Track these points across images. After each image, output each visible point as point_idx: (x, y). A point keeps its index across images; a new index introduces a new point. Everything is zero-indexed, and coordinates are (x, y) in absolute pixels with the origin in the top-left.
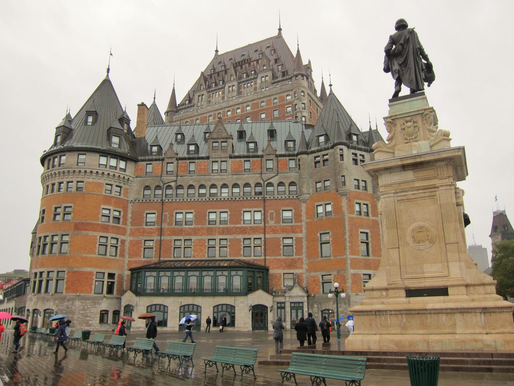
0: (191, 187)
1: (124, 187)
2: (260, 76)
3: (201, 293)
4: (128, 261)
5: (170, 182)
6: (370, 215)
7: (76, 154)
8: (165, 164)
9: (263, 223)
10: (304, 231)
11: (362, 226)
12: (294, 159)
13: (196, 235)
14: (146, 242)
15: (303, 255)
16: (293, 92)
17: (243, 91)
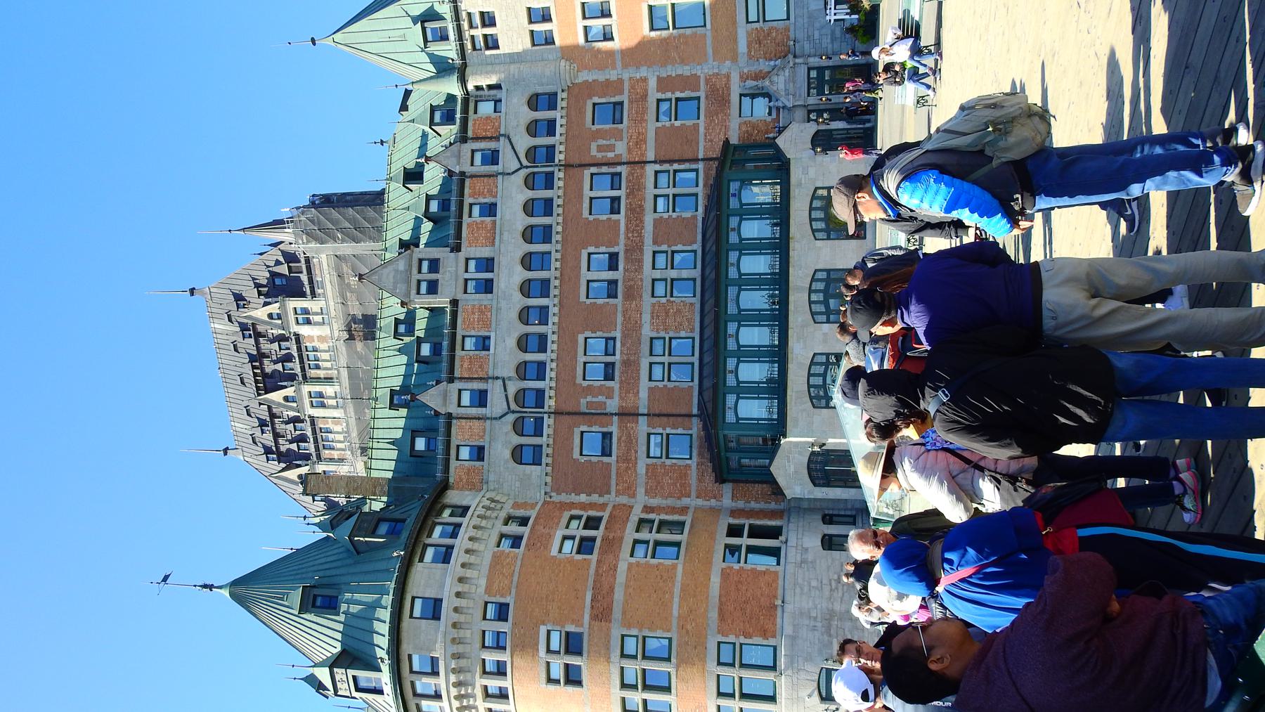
0: (523, 344)
1: (508, 509)
2: (295, 328)
3: (779, 281)
4: (697, 497)
5: (506, 396)
7: (406, 622)
8: (461, 411)
9: (618, 169)
10: (643, 72)
12: (476, 102)
14: (652, 454)
15: (699, 74)
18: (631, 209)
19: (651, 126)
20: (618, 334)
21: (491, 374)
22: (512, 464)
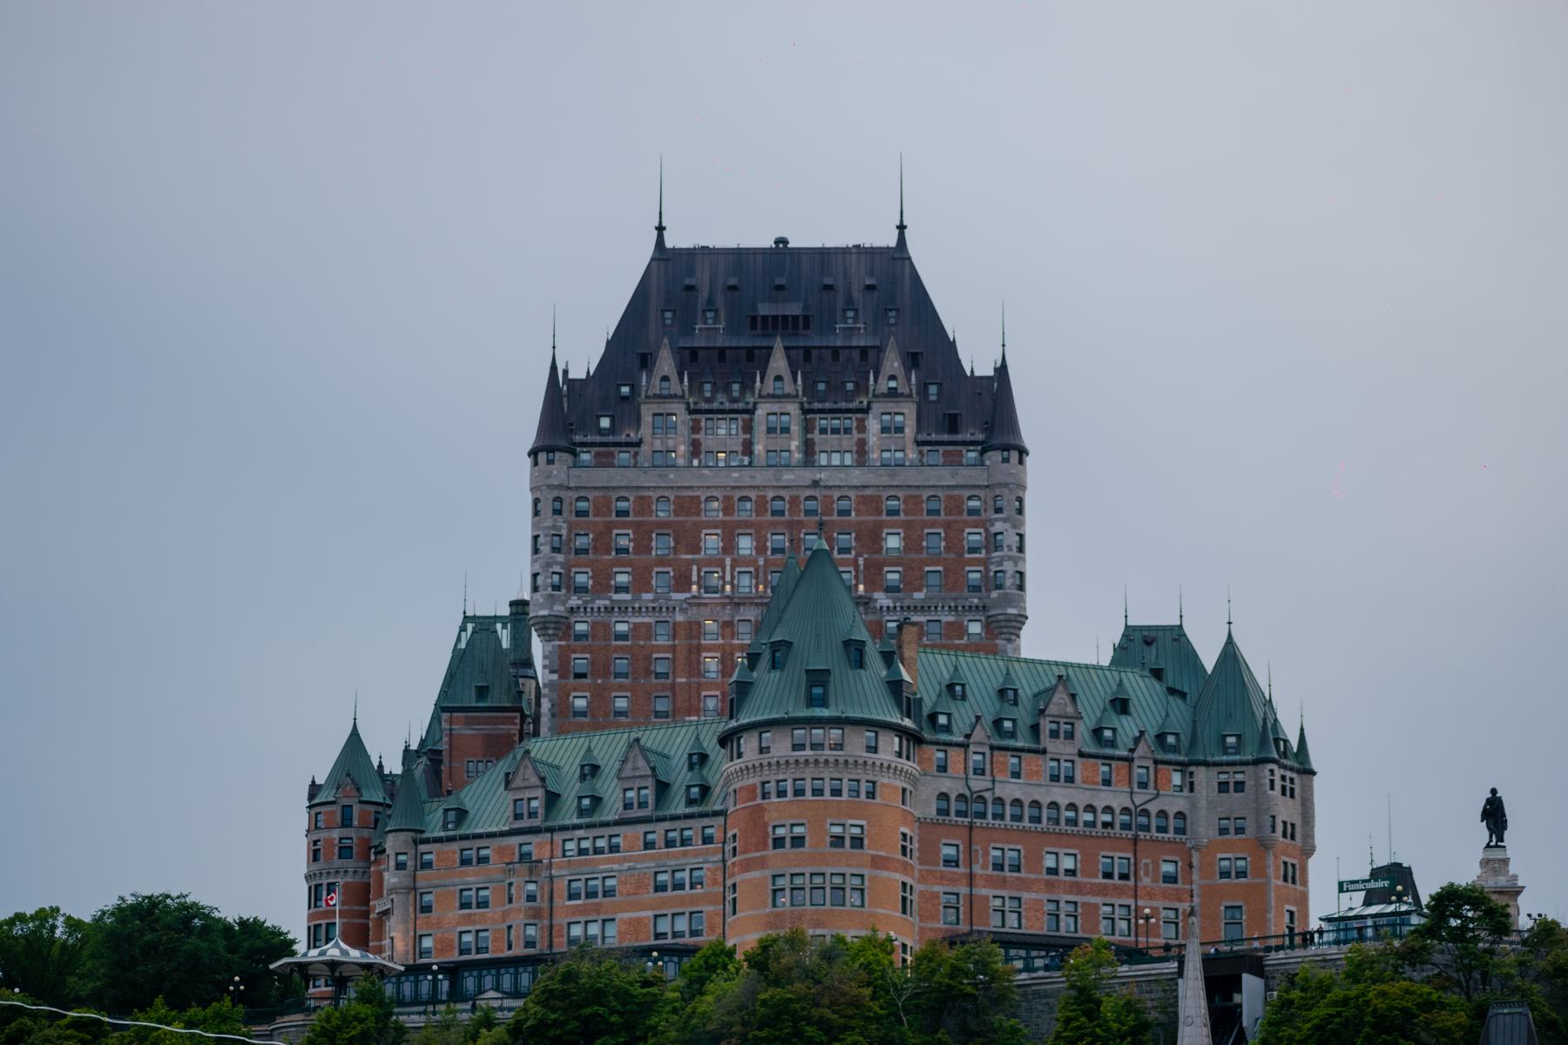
0: (1017, 802)
2: (877, 408)
4: (920, 928)
6: (1298, 882)
8: (971, 753)
9: (1132, 879)
11: (1288, 901)
12: (1181, 771)
13: (1028, 891)
17: (816, 440)
18: (1105, 886)
20: (1023, 874)
21: (997, 778)
22: (937, 793)
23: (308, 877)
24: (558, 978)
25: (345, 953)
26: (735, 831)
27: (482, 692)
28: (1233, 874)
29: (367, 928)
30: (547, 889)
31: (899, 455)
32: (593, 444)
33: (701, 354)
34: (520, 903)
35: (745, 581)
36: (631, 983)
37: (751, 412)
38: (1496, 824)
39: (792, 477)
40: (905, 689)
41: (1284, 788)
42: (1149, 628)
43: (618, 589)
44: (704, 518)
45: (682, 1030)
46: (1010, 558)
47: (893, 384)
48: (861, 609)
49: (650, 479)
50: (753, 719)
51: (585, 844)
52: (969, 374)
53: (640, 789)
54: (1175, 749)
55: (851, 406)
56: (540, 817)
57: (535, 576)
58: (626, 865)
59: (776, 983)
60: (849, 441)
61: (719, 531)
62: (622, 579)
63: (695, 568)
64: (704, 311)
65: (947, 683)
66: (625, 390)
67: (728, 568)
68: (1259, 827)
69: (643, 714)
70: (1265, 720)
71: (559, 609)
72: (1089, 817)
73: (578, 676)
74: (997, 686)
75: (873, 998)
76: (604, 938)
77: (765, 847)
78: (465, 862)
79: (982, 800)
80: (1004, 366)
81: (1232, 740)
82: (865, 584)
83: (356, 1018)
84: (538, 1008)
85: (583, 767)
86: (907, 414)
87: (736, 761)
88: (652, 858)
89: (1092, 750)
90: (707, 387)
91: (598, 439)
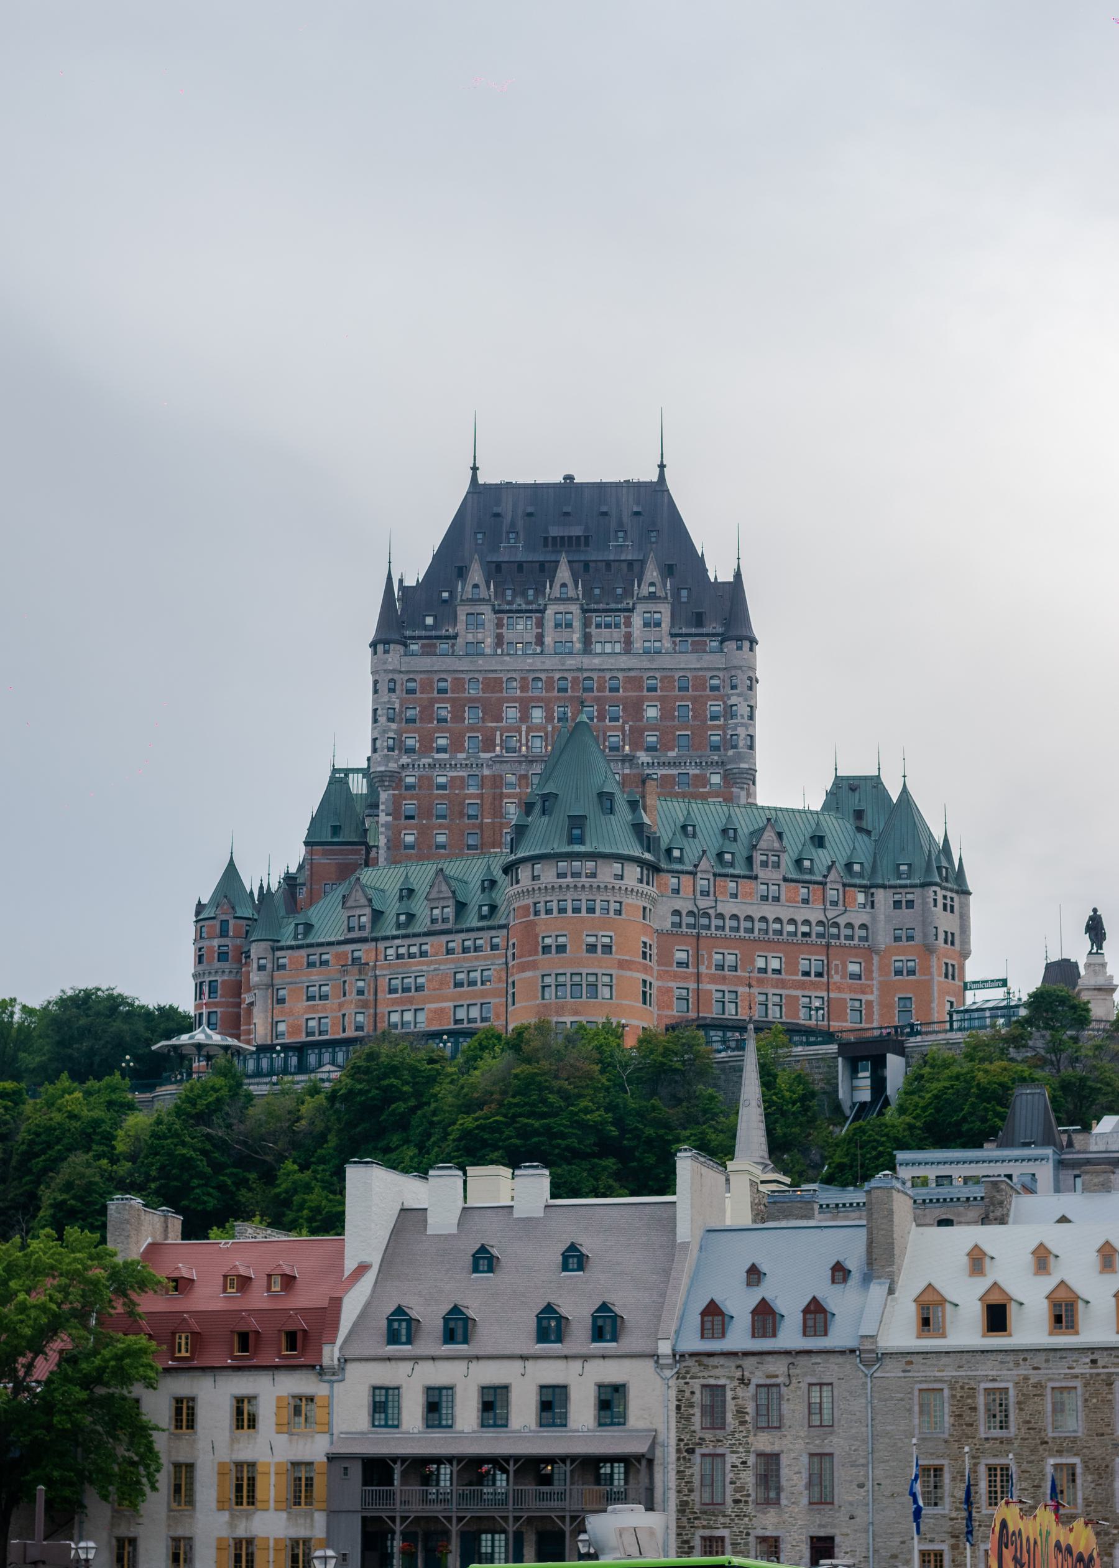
0: (734, 917)
2: (640, 608)
10: (876, 992)
11: (948, 994)
16: (727, 676)
18: (804, 982)
19: (847, 996)
20: (739, 973)
23: (195, 976)
24: (363, 1057)
25: (208, 1037)
26: (514, 940)
27: (336, 830)
28: (905, 973)
29: (238, 1015)
30: (372, 985)
31: (657, 644)
32: (420, 638)
33: (503, 565)
34: (352, 996)
35: (537, 743)
36: (419, 1061)
37: (542, 611)
38: (1096, 935)
39: (573, 662)
40: (645, 829)
41: (945, 905)
42: (854, 778)
43: (440, 750)
44: (505, 694)
45: (457, 1096)
46: (743, 725)
47: (652, 589)
48: (627, 765)
49: (464, 664)
50: (527, 854)
51: (402, 951)
52: (713, 580)
53: (443, 907)
54: (861, 875)
55: (619, 606)
56: (368, 930)
57: (374, 740)
58: (432, 967)
59: (528, 1061)
60: (618, 634)
61: (517, 705)
62: (442, 742)
63: (498, 733)
64: (508, 533)
65: (679, 824)
66: (445, 595)
67: (524, 733)
68: (925, 935)
69: (459, 848)
70: (930, 851)
71: (393, 766)
72: (791, 928)
73: (408, 818)
74: (721, 827)
75: (602, 1072)
76: (416, 1023)
77: (536, 953)
78: (310, 965)
79: (707, 915)
80: (738, 575)
81: (904, 868)
82: (630, 745)
83: (213, 1089)
84: (348, 1081)
85: (401, 890)
86: (664, 612)
87: (515, 886)
88: (452, 961)
89: (794, 876)
90: (509, 592)
91: (424, 633)
